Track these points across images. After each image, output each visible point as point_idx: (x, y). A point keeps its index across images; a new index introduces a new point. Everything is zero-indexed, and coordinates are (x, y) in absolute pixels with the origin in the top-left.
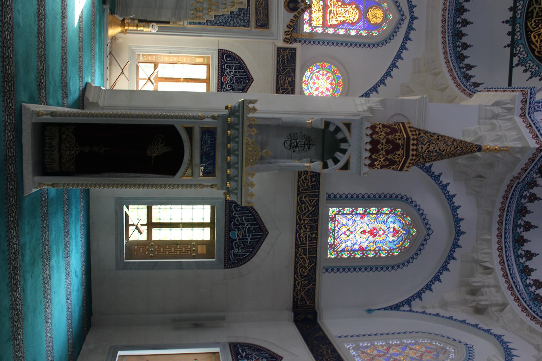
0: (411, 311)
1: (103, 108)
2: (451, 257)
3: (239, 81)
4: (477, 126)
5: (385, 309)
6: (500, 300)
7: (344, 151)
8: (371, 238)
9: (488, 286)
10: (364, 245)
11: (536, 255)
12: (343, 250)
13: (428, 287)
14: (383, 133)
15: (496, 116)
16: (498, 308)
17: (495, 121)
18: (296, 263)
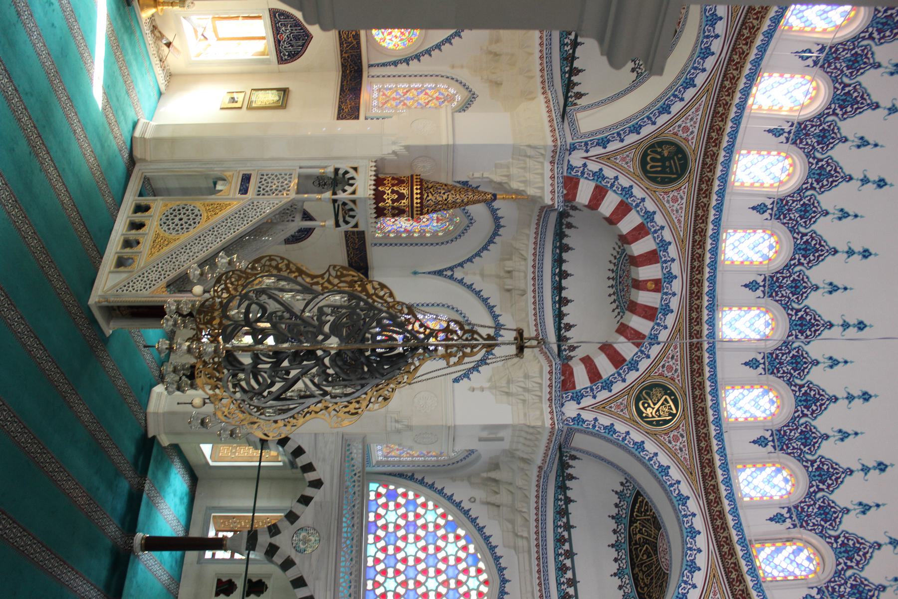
0: (451, 277)
1: (151, 162)
2: (491, 241)
3: (297, 38)
4: (511, 160)
5: (429, 273)
6: (522, 286)
7: (353, 217)
8: (415, 224)
9: (519, 271)
10: (409, 228)
11: (572, 249)
12: (389, 232)
13: (470, 260)
14: (389, 201)
15: (529, 157)
16: (520, 292)
17: (528, 160)
18: (347, 241)
